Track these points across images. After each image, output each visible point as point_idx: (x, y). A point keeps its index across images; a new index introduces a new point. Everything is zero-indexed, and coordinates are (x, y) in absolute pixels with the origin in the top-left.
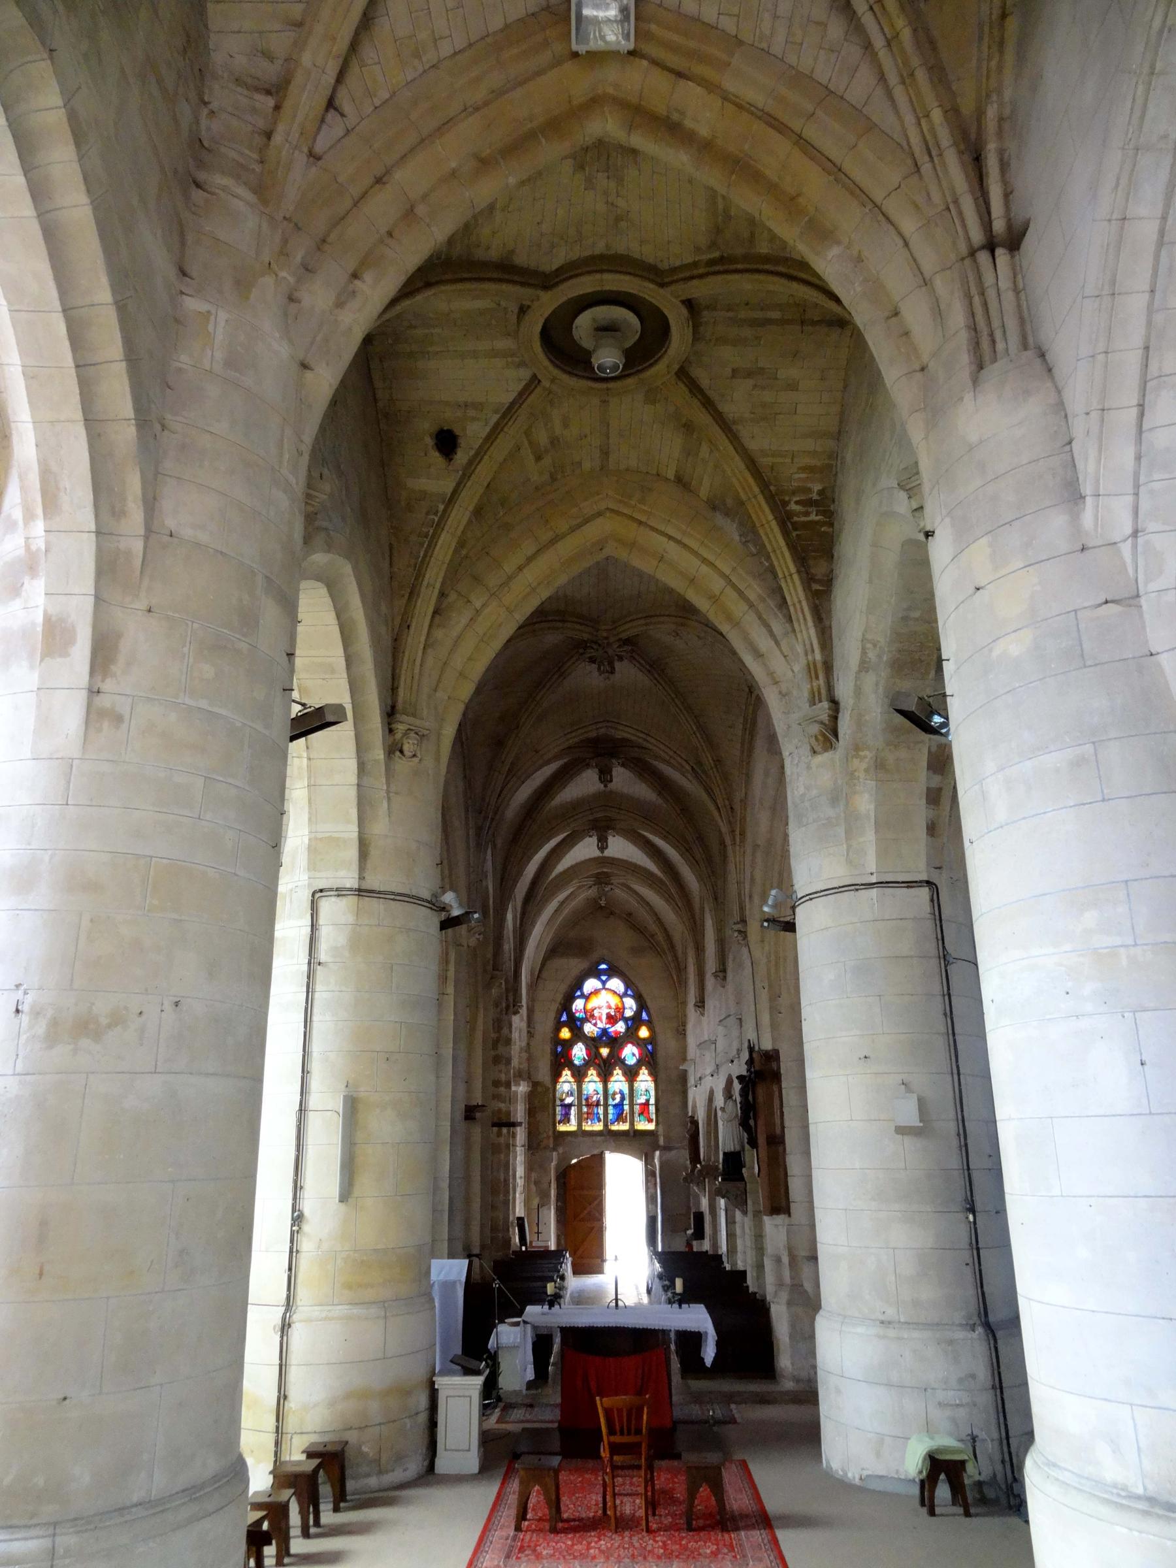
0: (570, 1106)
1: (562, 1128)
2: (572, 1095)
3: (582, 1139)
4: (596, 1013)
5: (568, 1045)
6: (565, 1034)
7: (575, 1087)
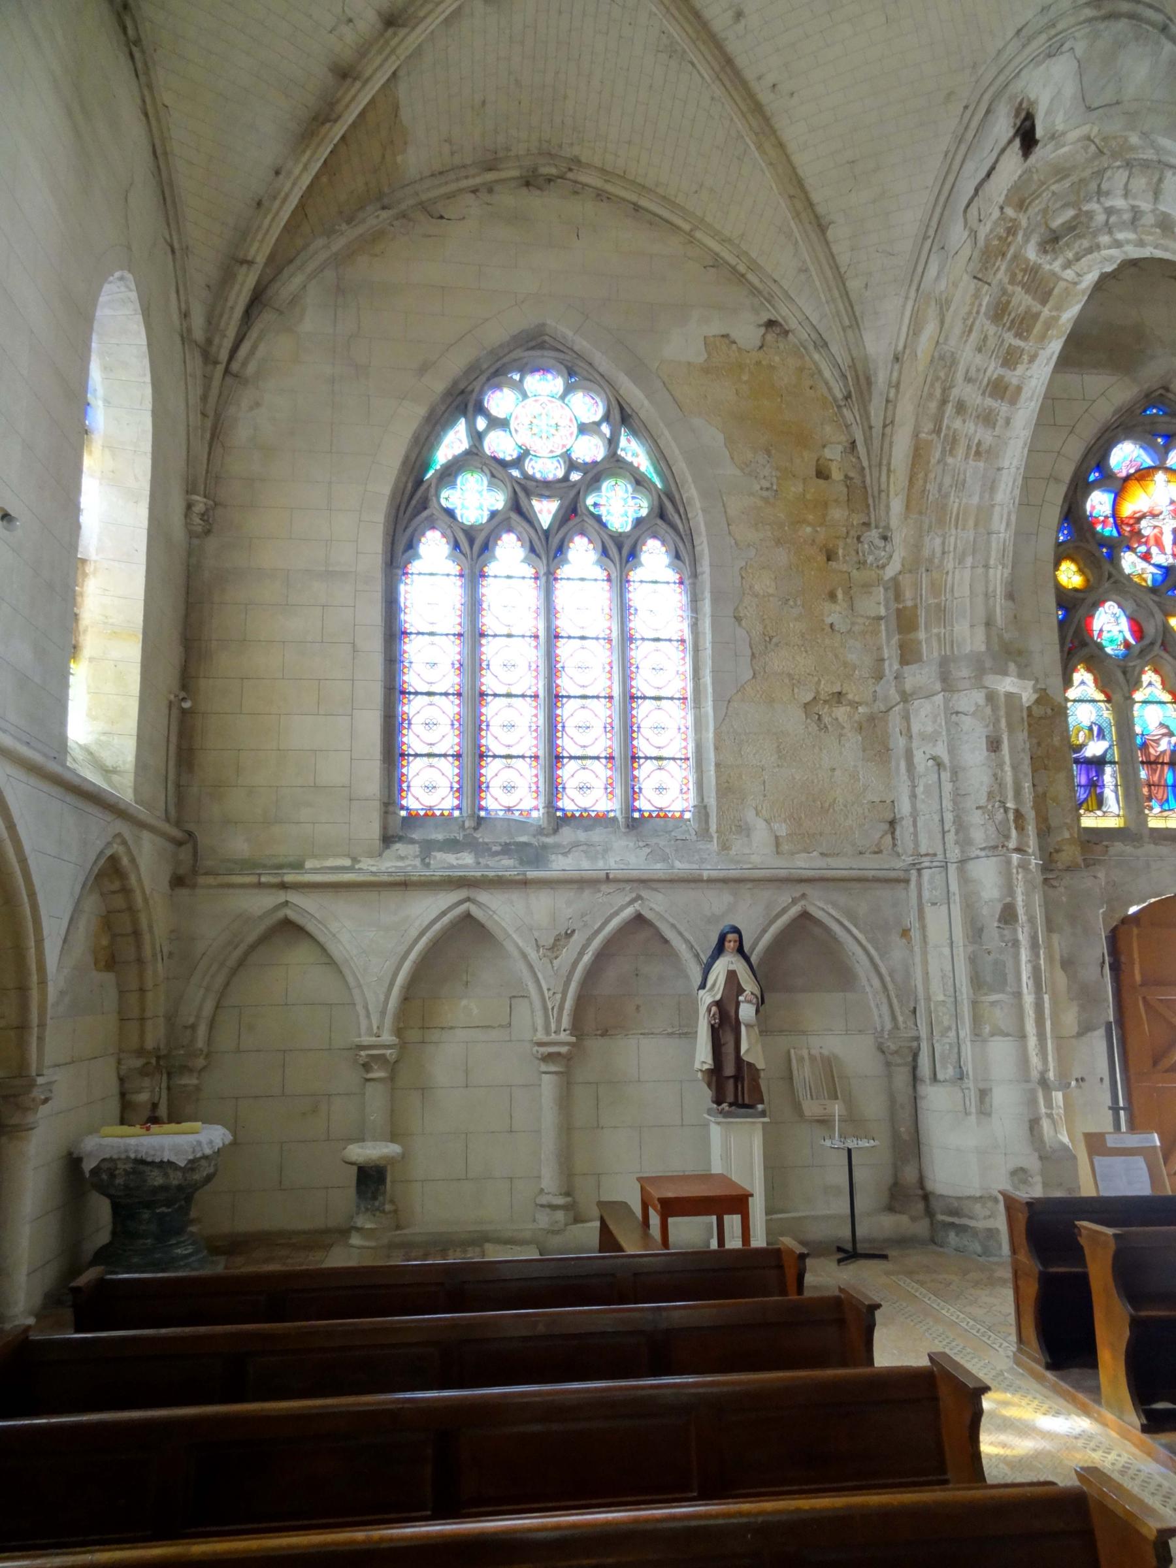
0: (1098, 763)
1: (1089, 821)
2: (1101, 734)
3: (1150, 848)
4: (1146, 527)
5: (1074, 607)
6: (1070, 576)
7: (1106, 714)
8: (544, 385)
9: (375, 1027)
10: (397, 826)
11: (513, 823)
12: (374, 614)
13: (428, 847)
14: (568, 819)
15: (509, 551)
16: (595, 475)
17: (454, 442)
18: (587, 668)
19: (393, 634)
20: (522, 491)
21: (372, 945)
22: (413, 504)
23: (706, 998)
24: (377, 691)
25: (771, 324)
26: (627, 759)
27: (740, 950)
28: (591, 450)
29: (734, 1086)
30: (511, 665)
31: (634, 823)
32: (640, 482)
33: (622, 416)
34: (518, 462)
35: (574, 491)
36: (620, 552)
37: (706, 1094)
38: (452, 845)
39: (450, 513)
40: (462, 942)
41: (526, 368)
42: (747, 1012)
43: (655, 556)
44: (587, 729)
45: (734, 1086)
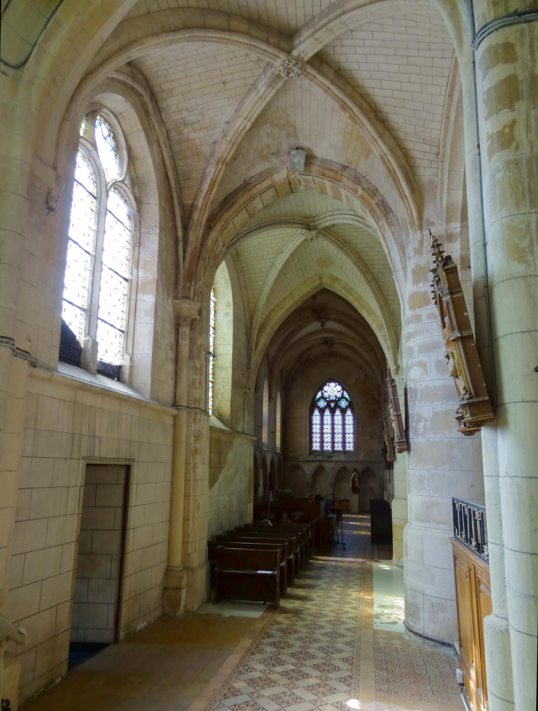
8: (332, 385)
9: (309, 479)
10: (312, 452)
11: (328, 451)
12: (308, 423)
13: (316, 456)
14: (336, 451)
15: (327, 412)
16: (340, 399)
17: (319, 395)
18: (338, 429)
19: (311, 424)
20: (329, 402)
21: (309, 469)
22: (313, 405)
23: (351, 478)
24: (308, 434)
25: (366, 375)
26: (344, 442)
27: (357, 472)
28: (339, 395)
29: (355, 490)
30: (327, 429)
31: (344, 452)
32: (347, 400)
33: (343, 389)
34: (329, 398)
35: (337, 401)
36: (343, 412)
37: (351, 491)
38: (319, 456)
39: (319, 407)
40: (320, 470)
41: (329, 383)
42: (356, 480)
43: (349, 412)
44: (338, 438)
45: (355, 490)
